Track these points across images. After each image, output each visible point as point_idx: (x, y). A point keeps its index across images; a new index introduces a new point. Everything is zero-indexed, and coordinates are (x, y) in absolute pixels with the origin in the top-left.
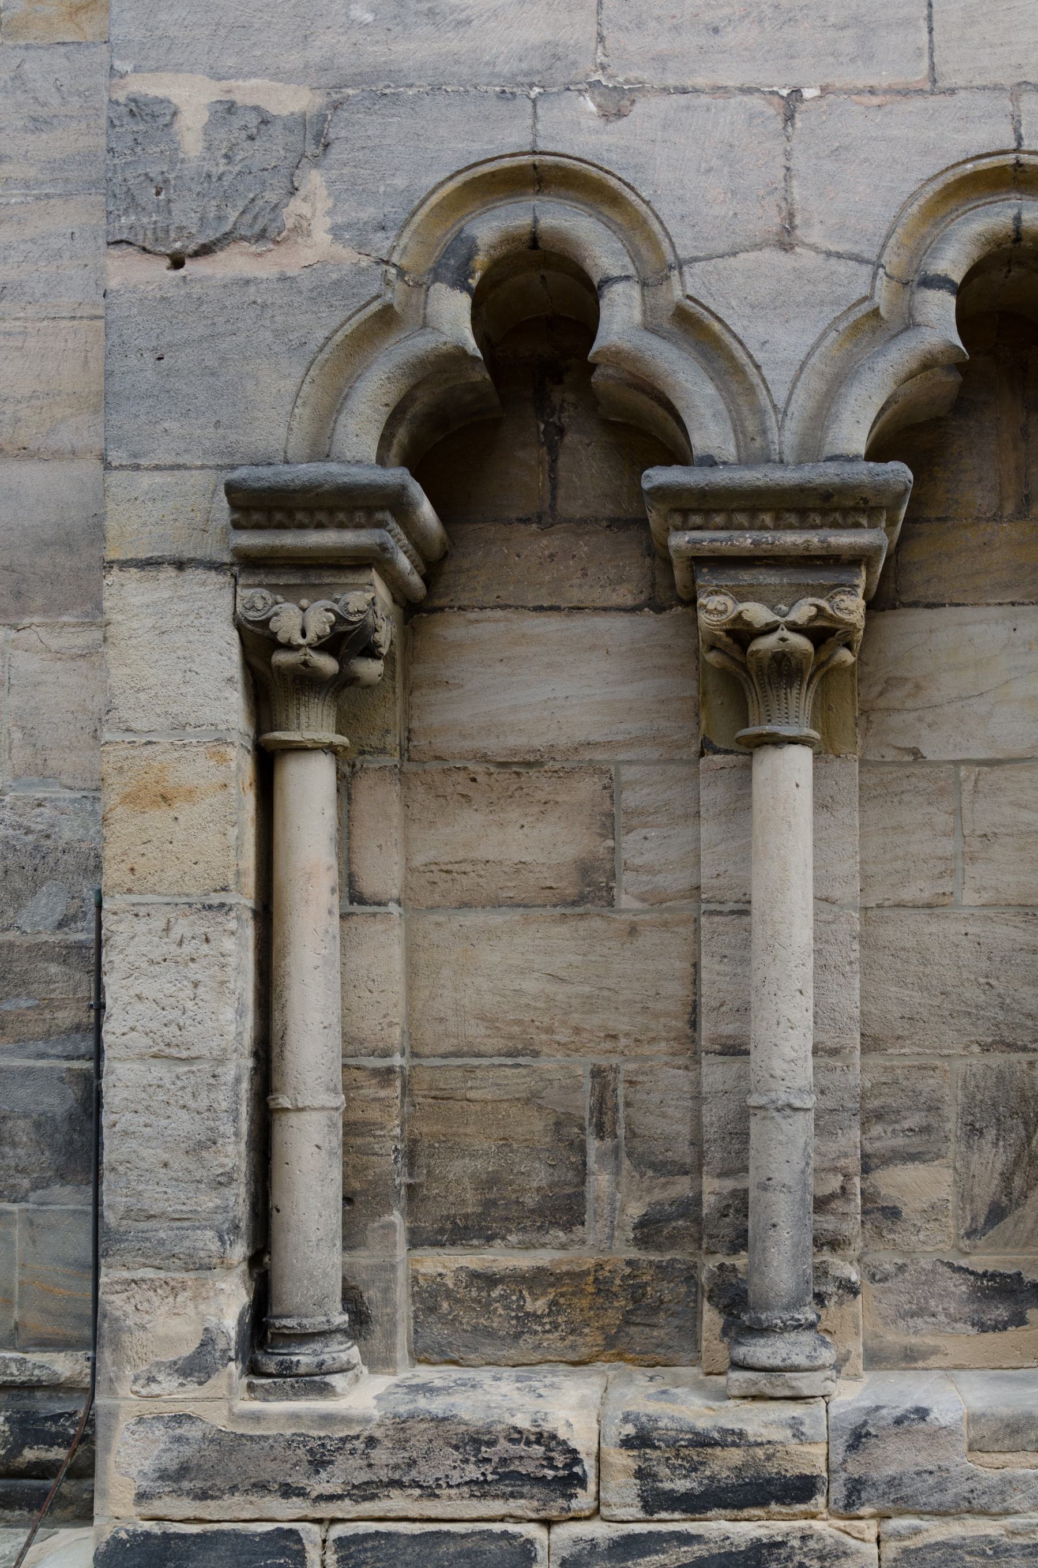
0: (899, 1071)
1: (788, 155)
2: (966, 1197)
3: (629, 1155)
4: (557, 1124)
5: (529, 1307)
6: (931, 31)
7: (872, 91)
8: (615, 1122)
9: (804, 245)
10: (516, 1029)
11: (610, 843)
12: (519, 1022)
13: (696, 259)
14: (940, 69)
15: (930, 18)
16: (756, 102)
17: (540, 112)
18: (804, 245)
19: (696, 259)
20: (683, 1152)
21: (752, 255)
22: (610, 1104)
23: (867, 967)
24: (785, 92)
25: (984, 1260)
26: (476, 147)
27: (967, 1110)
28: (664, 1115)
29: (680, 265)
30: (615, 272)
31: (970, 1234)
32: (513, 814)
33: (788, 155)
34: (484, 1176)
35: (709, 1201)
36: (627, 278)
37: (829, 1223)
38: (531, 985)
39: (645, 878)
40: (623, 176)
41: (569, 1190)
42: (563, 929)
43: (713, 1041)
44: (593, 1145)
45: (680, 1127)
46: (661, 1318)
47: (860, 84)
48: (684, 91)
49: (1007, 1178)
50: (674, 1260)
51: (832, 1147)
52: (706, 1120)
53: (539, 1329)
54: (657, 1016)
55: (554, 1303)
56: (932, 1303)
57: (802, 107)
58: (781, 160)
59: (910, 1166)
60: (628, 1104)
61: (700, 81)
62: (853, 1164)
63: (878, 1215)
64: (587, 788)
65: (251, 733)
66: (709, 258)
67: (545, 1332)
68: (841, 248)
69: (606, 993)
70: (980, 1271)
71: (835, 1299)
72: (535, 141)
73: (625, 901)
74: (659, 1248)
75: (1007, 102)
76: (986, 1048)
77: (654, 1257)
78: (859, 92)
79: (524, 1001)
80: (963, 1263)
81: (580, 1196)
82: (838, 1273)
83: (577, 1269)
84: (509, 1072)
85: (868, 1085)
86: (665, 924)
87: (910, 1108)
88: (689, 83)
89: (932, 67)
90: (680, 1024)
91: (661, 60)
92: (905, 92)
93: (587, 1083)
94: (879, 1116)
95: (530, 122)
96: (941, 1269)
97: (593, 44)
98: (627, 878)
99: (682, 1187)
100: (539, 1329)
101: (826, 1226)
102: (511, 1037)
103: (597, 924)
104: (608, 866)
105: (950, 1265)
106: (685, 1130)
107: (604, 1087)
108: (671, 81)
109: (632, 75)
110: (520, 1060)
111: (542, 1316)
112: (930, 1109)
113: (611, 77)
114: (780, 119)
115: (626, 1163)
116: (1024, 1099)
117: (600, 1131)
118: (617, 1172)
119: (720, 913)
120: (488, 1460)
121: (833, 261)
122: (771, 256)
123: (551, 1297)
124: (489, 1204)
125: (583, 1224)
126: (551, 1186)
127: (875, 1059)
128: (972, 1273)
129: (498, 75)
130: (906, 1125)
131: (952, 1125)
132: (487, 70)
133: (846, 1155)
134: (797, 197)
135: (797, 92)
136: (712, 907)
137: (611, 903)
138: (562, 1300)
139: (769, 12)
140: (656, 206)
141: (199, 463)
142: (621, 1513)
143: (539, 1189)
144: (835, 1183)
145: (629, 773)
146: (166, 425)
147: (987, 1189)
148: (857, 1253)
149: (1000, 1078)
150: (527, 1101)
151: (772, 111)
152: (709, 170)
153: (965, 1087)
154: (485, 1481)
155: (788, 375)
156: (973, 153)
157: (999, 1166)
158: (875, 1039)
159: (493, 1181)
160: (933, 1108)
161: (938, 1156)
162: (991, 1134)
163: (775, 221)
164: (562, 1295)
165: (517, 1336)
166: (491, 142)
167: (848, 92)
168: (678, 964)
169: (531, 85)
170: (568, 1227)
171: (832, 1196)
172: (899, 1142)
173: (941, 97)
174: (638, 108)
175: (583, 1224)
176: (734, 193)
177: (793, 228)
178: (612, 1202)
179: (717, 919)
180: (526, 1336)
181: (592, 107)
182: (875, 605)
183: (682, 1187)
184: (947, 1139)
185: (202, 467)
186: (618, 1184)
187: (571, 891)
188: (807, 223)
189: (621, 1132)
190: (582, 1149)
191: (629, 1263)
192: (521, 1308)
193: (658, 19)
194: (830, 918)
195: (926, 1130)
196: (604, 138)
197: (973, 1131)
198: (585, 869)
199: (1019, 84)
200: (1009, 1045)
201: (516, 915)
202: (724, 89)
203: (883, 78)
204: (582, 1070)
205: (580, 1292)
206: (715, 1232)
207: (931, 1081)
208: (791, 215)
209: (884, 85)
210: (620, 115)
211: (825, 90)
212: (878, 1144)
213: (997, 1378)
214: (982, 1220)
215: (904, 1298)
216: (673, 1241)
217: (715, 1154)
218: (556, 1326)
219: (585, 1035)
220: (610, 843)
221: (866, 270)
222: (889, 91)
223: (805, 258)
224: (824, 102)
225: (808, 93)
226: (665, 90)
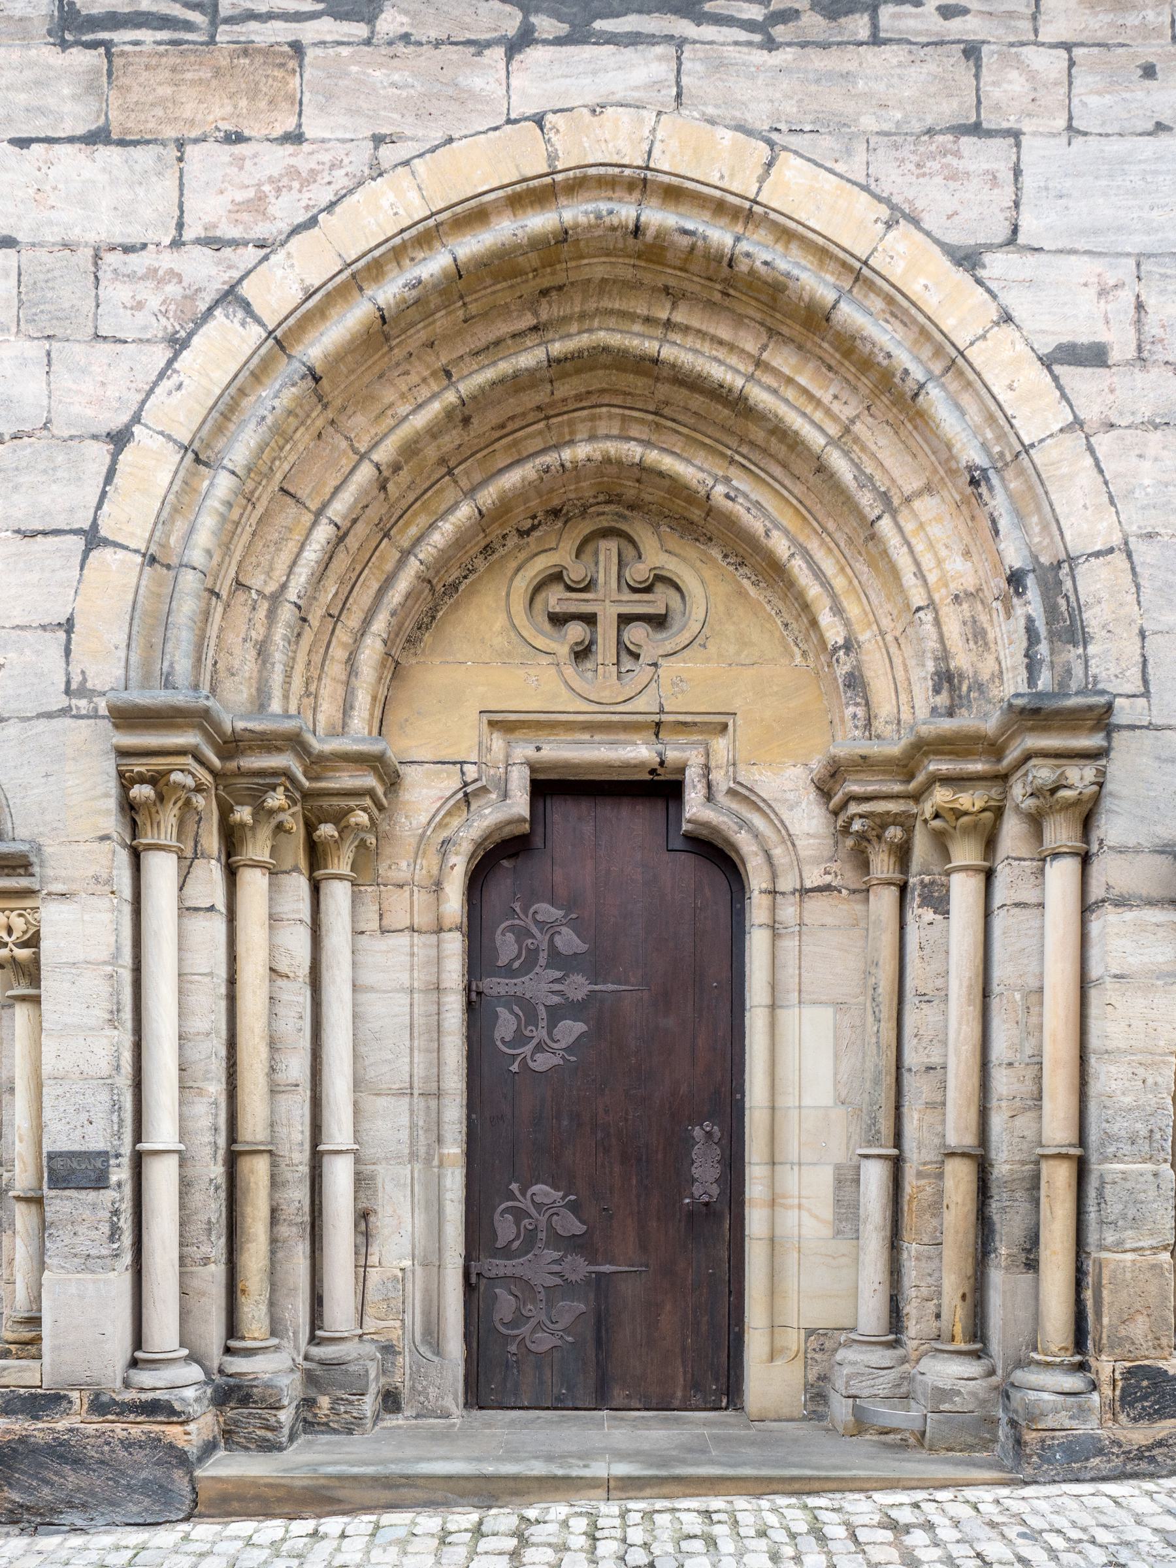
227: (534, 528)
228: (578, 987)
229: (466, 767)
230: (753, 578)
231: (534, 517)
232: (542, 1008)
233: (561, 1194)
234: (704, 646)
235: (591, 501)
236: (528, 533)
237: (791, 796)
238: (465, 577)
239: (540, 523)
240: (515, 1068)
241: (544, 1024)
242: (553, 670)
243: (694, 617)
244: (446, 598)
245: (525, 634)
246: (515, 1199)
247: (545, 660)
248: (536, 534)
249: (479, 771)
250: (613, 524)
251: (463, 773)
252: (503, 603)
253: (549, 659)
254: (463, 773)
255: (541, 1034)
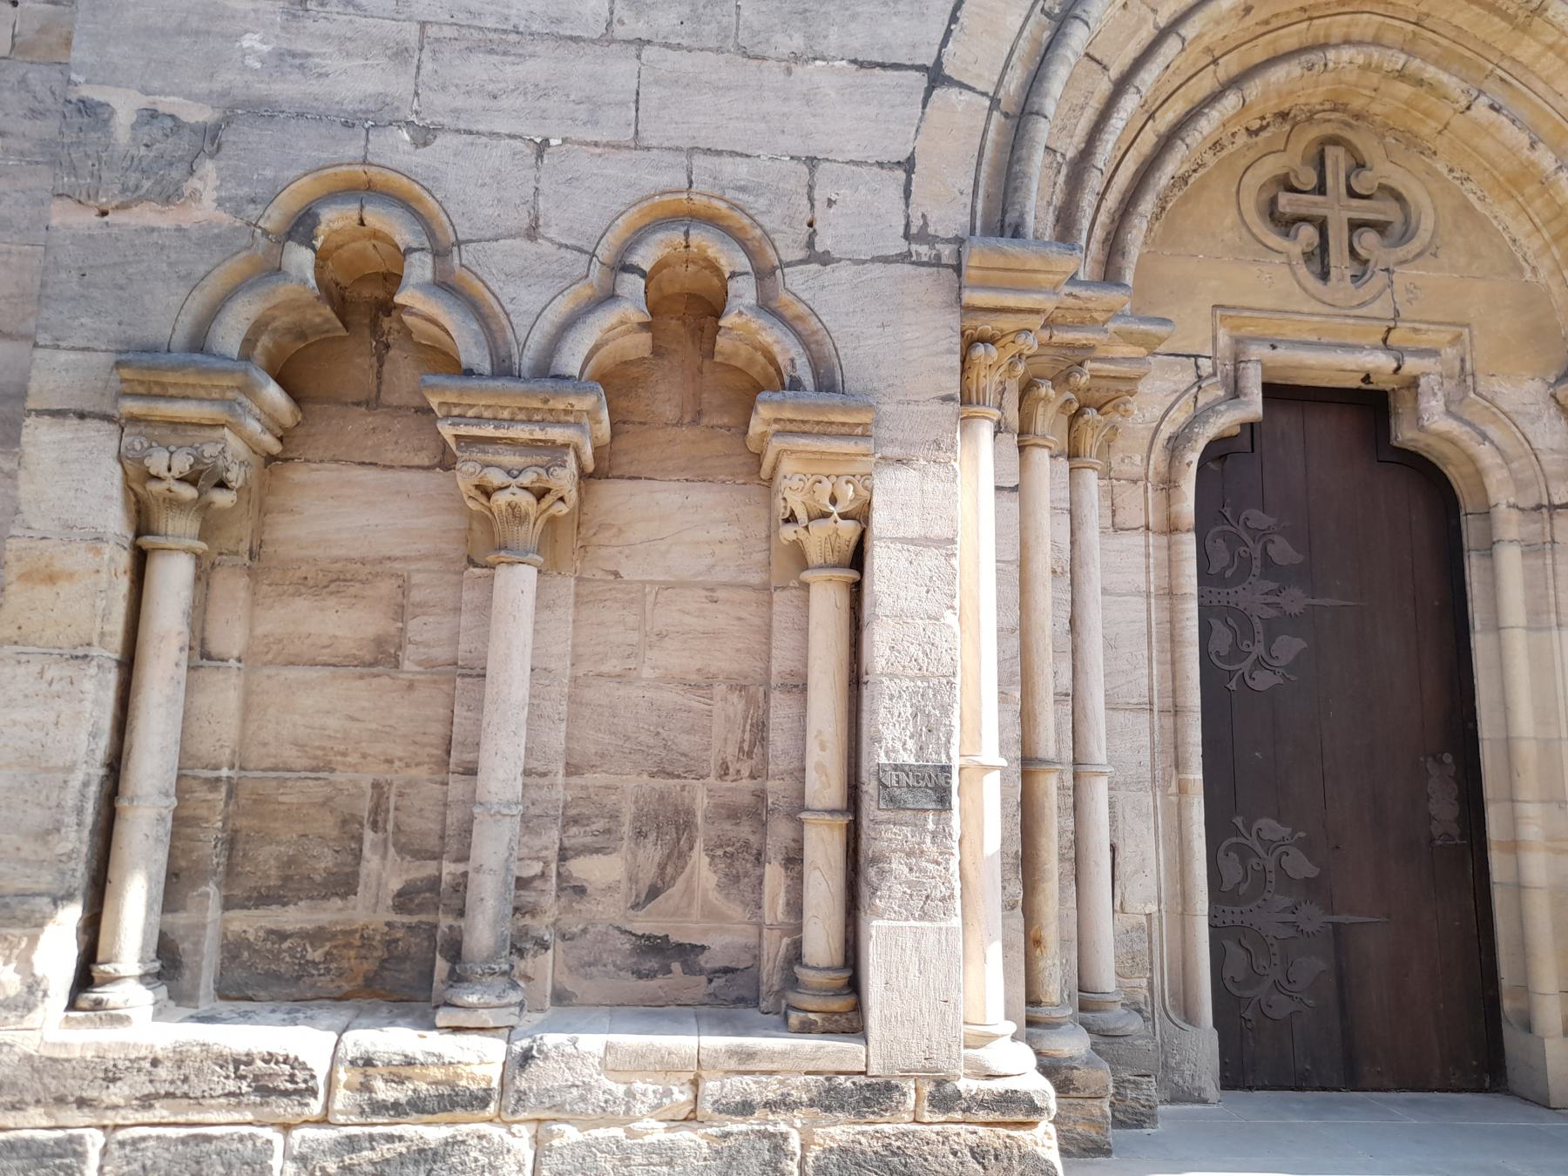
0: (591, 790)
1: (537, 180)
2: (632, 879)
3: (394, 845)
4: (344, 822)
5: (309, 957)
6: (637, 110)
7: (596, 144)
8: (386, 821)
9: (544, 237)
10: (320, 753)
11: (400, 625)
12: (323, 749)
13: (470, 241)
14: (640, 135)
15: (637, 101)
16: (518, 144)
17: (371, 137)
18: (544, 237)
19: (470, 241)
20: (433, 843)
21: (509, 242)
22: (383, 808)
23: (572, 719)
24: (538, 140)
25: (645, 924)
26: (324, 155)
27: (637, 818)
28: (422, 817)
29: (459, 243)
30: (415, 245)
31: (635, 906)
32: (331, 602)
33: (537, 180)
34: (286, 859)
35: (446, 878)
36: (423, 249)
37: (529, 897)
38: (333, 723)
39: (422, 650)
40: (425, 184)
41: (348, 869)
42: (361, 683)
43: (457, 765)
44: (369, 835)
45: (431, 826)
46: (408, 965)
47: (589, 139)
48: (471, 133)
49: (662, 868)
50: (422, 922)
51: (537, 843)
52: (448, 822)
53: (315, 972)
54: (424, 745)
55: (328, 953)
56: (605, 956)
57: (550, 150)
58: (533, 183)
59: (595, 856)
60: (397, 809)
61: (481, 128)
62: (552, 854)
63: (570, 891)
64: (386, 587)
65: (130, 536)
66: (480, 241)
67: (320, 975)
68: (568, 243)
69: (387, 729)
70: (640, 933)
71: (532, 952)
72: (366, 156)
73: (407, 665)
74: (410, 912)
75: (684, 159)
76: (652, 775)
77: (406, 919)
78: (587, 144)
79: (327, 733)
80: (628, 927)
81: (356, 874)
82: (535, 934)
83: (348, 928)
84: (311, 783)
85: (569, 799)
86: (435, 682)
87: (597, 816)
88: (474, 129)
89: (637, 132)
90: (439, 752)
91: (456, 112)
92: (617, 147)
93: (369, 792)
94: (575, 821)
95: (363, 143)
96: (612, 932)
97: (411, 98)
98: (410, 649)
99: (429, 869)
100: (315, 972)
101: (529, 899)
102: (316, 758)
103: (385, 680)
104: (397, 640)
105: (618, 928)
106: (436, 827)
107: (381, 795)
108: (462, 126)
109: (436, 120)
110: (321, 775)
111: (320, 963)
112: (611, 817)
113: (423, 119)
114: (534, 156)
115: (392, 850)
116: (677, 812)
117: (375, 826)
118: (384, 857)
119: (470, 676)
120: (243, 1077)
121: (563, 250)
122: (520, 243)
123: (327, 948)
124: (287, 879)
125: (355, 894)
126: (336, 865)
127: (575, 780)
128: (634, 935)
129: (345, 111)
130: (594, 827)
131: (626, 830)
132: (337, 107)
133: (546, 848)
134: (541, 207)
135: (546, 141)
136: (464, 671)
137: (397, 665)
138: (335, 952)
139: (531, 88)
140: (446, 205)
141: (104, 348)
142: (342, 1119)
143: (325, 869)
144: (536, 868)
145: (416, 578)
146: (83, 320)
147: (648, 875)
148: (552, 920)
149: (662, 797)
150: (323, 804)
151: (529, 151)
152: (483, 185)
153: (636, 802)
154: (241, 1094)
155: (528, 321)
156: (661, 188)
157: (657, 859)
158: (576, 766)
159: (291, 861)
160: (614, 817)
161: (615, 850)
162: (652, 837)
163: (526, 222)
164: (336, 947)
165: (299, 978)
166: (336, 153)
167: (581, 143)
168: (441, 711)
169: (367, 121)
170: (344, 896)
171: (534, 878)
172: (589, 839)
173: (640, 152)
174: (438, 142)
175: (355, 894)
176: (499, 201)
177: (537, 226)
178: (379, 876)
179: (467, 680)
180: (305, 979)
181: (407, 137)
182: (586, 477)
183: (429, 869)
184: (622, 839)
185: (106, 351)
186: (384, 868)
187: (368, 658)
188: (547, 225)
189: (390, 827)
190: (359, 839)
191: (388, 924)
192: (303, 957)
193: (457, 86)
194: (547, 682)
195: (608, 831)
196: (414, 158)
197: (640, 834)
198: (379, 642)
199: (693, 148)
200: (668, 774)
201: (327, 671)
202: (498, 135)
203: (604, 136)
204: (366, 784)
205: (348, 946)
206: (448, 902)
207: (613, 797)
208: (537, 218)
209: (604, 140)
210: (425, 144)
211: (564, 140)
212: (573, 841)
213: (644, 1014)
214: (643, 896)
215: (584, 952)
216: (421, 908)
217: (453, 846)
218: (328, 970)
219: (369, 758)
220: (400, 625)
221: (586, 257)
222: (608, 145)
223: (545, 247)
224: (563, 148)
225: (553, 142)
226: (458, 131)
227: (1262, 128)
228: (1295, 600)
229: (1201, 361)
230: (1479, 193)
231: (1263, 118)
232: (1257, 620)
233: (1289, 830)
234: (1435, 255)
235: (1318, 107)
236: (1256, 133)
237: (1532, 409)
238: (1195, 171)
239: (1268, 124)
240: (1233, 685)
241: (1260, 637)
242: (1286, 269)
243: (1422, 227)
244: (1176, 190)
245: (1255, 230)
246: (1238, 833)
247: (1278, 259)
248: (1264, 135)
249: (1214, 364)
250: (1338, 132)
251: (1197, 367)
252: (1234, 199)
253: (1283, 258)
254: (1197, 367)
255: (1259, 649)
